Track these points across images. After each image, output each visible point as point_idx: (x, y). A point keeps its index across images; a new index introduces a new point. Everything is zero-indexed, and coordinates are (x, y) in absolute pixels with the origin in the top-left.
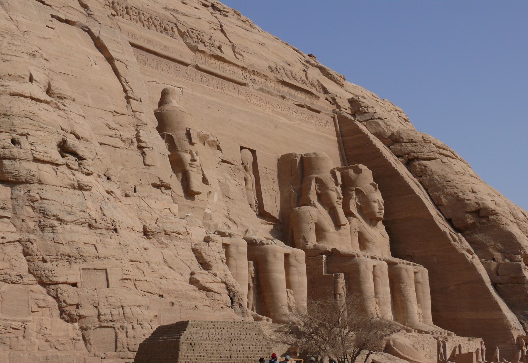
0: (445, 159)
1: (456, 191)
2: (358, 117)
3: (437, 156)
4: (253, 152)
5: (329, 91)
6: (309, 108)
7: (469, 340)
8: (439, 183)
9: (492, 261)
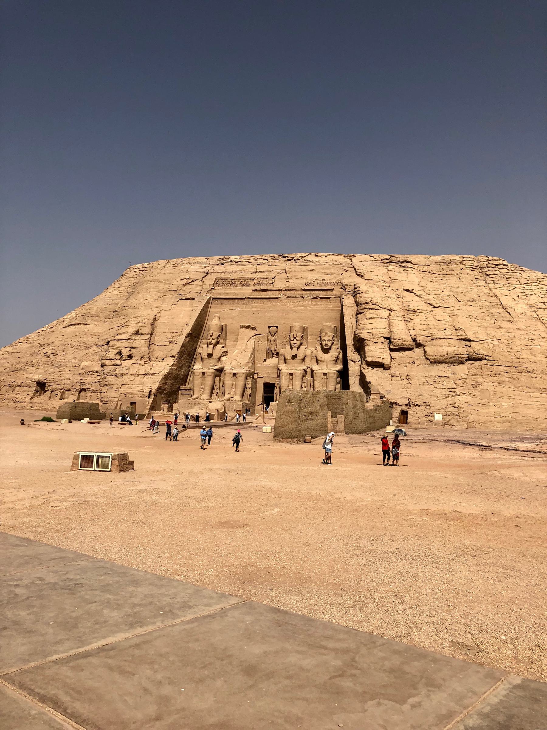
3: (364, 311)
4: (277, 327)
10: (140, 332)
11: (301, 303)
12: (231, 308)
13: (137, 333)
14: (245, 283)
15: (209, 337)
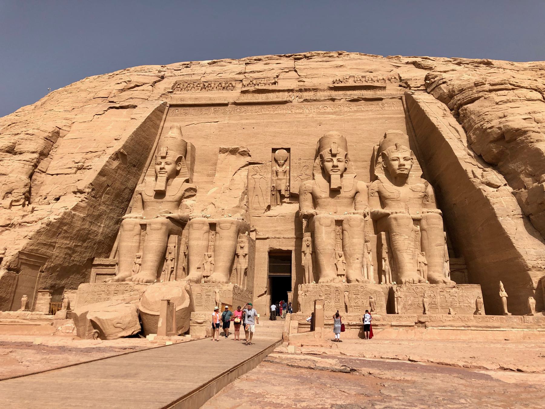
0: (493, 95)
1: (482, 123)
2: (429, 90)
3: (481, 94)
4: (288, 150)
5: (402, 78)
6: (366, 100)
7: (454, 287)
8: (474, 121)
9: (523, 190)
10: (17, 148)
11: (329, 110)
12: (203, 120)
13: (11, 150)
14: (227, 86)
15: (159, 160)
